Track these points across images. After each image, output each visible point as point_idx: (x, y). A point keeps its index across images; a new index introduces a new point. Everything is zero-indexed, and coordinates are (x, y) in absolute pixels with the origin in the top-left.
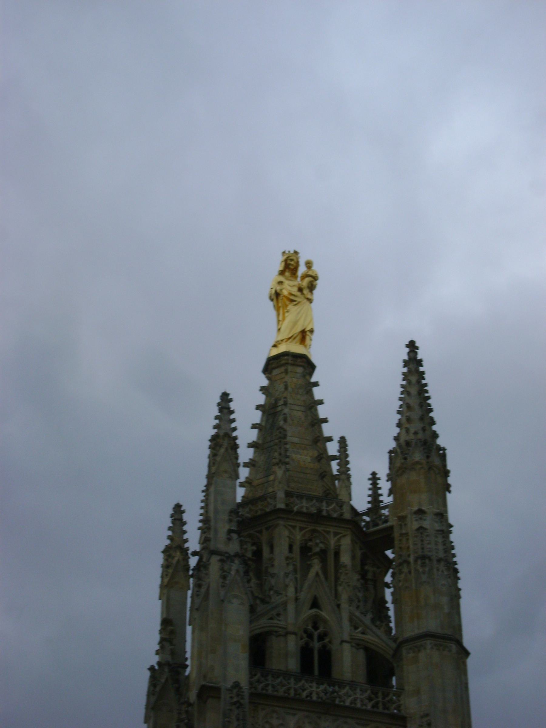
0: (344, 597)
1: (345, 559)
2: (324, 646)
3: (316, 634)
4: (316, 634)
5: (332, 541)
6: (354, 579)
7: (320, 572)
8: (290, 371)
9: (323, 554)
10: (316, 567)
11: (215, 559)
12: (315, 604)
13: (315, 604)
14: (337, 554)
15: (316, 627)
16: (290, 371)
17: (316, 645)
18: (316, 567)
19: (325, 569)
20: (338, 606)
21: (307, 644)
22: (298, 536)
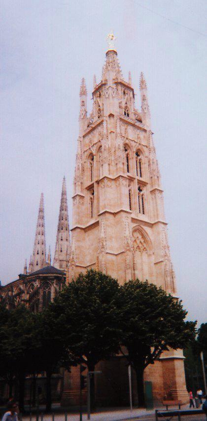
13: (126, 104)
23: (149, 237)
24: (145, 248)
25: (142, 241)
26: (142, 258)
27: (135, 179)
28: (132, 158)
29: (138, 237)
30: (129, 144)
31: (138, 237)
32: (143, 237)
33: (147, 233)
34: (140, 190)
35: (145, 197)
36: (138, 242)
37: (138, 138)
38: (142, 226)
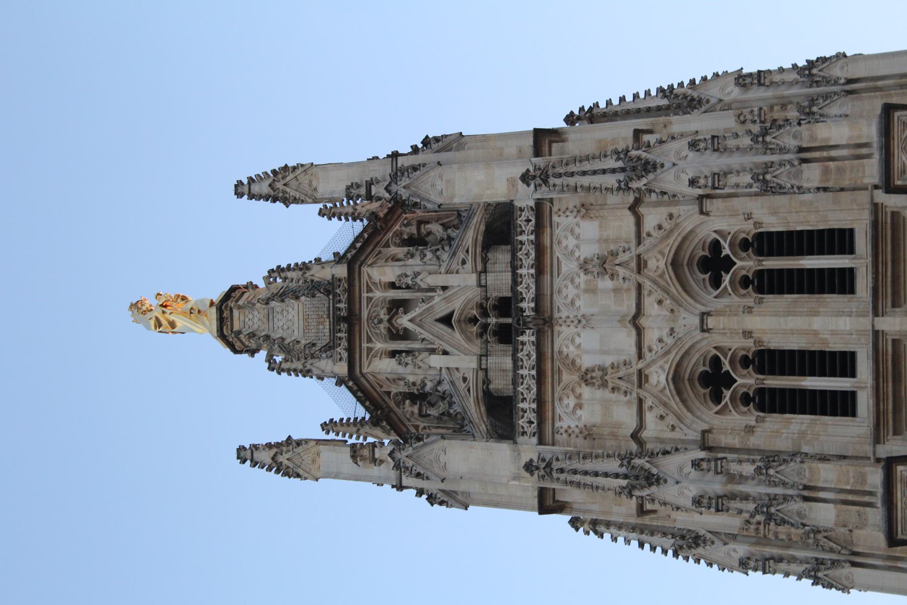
0: (431, 281)
2: (495, 307)
3: (482, 320)
4: (482, 320)
5: (378, 294)
6: (415, 263)
7: (410, 316)
10: (404, 321)
11: (406, 481)
12: (446, 320)
13: (446, 320)
14: (393, 286)
15: (474, 320)
17: (492, 320)
18: (404, 321)
20: (444, 288)
21: (495, 333)
22: (379, 345)
28: (747, 334)
30: (674, 357)
37: (603, 265)
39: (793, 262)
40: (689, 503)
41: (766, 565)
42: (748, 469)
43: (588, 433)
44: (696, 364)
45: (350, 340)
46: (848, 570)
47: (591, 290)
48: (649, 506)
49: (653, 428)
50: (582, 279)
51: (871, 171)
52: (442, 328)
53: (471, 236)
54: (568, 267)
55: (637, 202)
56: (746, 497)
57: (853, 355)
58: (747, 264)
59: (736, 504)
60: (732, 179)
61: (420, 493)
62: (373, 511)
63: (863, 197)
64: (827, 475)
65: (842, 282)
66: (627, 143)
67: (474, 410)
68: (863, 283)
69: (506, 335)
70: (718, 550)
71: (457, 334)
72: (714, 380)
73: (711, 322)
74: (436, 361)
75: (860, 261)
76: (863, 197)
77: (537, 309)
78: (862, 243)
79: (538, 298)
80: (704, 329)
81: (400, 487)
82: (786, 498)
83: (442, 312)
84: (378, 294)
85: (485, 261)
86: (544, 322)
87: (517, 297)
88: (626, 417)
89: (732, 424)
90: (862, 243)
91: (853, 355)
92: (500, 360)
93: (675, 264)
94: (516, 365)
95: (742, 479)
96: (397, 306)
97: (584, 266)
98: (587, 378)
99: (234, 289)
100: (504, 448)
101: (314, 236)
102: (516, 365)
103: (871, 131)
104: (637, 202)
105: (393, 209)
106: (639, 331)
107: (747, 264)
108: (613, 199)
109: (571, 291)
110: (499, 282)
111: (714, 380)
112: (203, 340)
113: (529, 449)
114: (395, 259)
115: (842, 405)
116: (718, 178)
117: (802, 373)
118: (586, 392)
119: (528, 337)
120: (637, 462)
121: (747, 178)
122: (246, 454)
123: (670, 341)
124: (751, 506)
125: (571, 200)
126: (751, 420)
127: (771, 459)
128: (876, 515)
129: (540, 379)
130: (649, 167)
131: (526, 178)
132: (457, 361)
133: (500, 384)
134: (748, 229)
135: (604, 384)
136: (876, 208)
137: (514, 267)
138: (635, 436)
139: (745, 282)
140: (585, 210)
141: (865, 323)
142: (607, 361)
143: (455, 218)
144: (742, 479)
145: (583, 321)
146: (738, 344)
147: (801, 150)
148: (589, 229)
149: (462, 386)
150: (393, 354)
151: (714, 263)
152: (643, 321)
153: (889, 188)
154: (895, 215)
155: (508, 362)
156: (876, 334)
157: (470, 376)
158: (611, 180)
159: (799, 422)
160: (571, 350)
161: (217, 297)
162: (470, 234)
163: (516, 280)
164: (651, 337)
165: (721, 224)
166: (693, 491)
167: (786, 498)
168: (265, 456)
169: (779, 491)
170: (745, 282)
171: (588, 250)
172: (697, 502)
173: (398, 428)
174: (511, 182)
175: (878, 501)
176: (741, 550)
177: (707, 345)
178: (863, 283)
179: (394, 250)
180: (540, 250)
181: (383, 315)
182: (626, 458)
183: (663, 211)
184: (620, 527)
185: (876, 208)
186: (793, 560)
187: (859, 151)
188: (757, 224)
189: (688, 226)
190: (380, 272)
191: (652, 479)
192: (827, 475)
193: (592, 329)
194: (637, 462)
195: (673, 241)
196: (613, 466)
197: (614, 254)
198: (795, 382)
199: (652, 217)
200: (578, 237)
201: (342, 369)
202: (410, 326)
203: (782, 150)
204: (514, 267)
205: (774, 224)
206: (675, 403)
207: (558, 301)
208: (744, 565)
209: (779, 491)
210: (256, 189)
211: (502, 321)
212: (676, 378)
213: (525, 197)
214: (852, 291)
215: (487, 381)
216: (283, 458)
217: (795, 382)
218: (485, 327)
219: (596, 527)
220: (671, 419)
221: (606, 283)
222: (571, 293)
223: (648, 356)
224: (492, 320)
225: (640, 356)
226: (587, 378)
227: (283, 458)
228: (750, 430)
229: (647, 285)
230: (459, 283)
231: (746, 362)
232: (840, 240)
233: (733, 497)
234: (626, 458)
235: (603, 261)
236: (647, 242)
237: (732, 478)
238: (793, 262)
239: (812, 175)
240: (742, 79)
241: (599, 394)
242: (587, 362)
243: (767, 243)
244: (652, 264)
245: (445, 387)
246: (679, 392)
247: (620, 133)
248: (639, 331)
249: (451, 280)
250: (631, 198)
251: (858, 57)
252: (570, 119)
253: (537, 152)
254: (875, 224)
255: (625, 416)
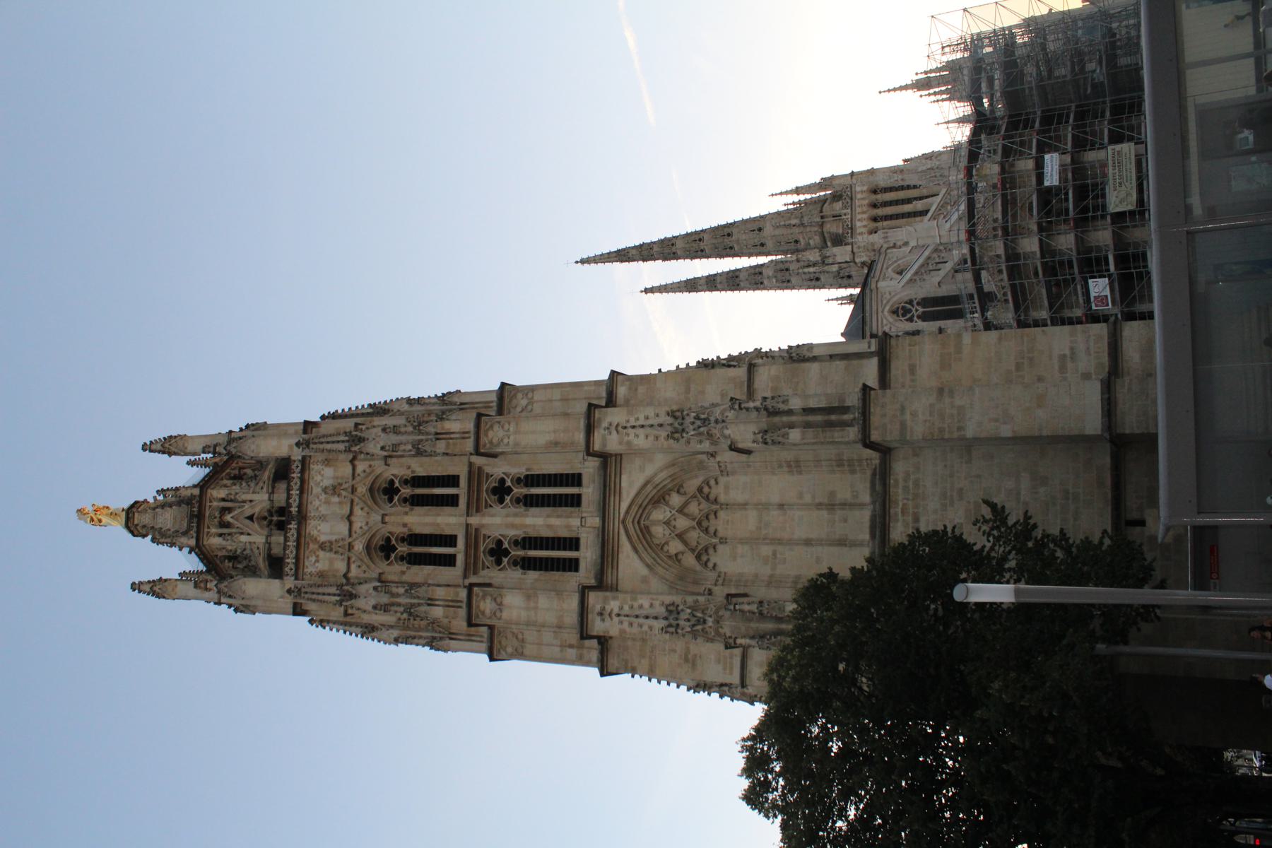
0: (244, 497)
1: (222, 493)
5: (215, 504)
6: (236, 488)
8: (136, 519)
9: (224, 510)
10: (228, 518)
12: (251, 518)
13: (251, 518)
14: (223, 500)
15: (265, 518)
16: (136, 519)
18: (228, 518)
19: (229, 510)
22: (213, 530)
23: (656, 474)
24: (700, 490)
25: (676, 500)
26: (744, 506)
27: (467, 525)
28: (405, 525)
29: (667, 523)
30: (367, 536)
31: (667, 523)
32: (660, 499)
33: (645, 485)
34: (501, 491)
35: (521, 471)
36: (682, 523)
37: (334, 490)
38: (624, 506)
39: (429, 491)
40: (370, 609)
41: (407, 640)
42: (401, 590)
43: (321, 575)
44: (379, 541)
45: (198, 527)
46: (447, 641)
47: (327, 502)
48: (350, 611)
49: (354, 572)
50: (323, 497)
51: (469, 445)
52: (248, 522)
53: (267, 474)
54: (317, 490)
55: (354, 458)
56: (399, 605)
57: (455, 537)
58: (406, 491)
59: (394, 608)
60: (402, 447)
61: (230, 606)
62: (205, 617)
63: (465, 459)
64: (440, 593)
65: (452, 501)
66: (352, 430)
67: (262, 563)
68: (463, 501)
69: (281, 526)
70: (385, 634)
71: (256, 525)
72: (387, 549)
73: (387, 519)
74: (244, 538)
75: (461, 491)
76: (465, 459)
77: (299, 512)
78: (463, 482)
79: (300, 506)
80: (383, 522)
81: (219, 603)
82: (419, 605)
83: (248, 513)
84: (215, 504)
85: (273, 487)
86: (302, 517)
87: (289, 505)
88: (341, 566)
89: (394, 570)
90: (463, 482)
91: (455, 537)
92: (278, 538)
93: (371, 490)
94: (286, 539)
95: (398, 595)
96: (224, 510)
97: (325, 490)
98: (322, 547)
99: (136, 502)
100: (276, 583)
101: (182, 473)
102: (286, 539)
103: (470, 426)
104: (354, 458)
105: (228, 459)
106: (351, 524)
107: (406, 491)
108: (342, 456)
109: (317, 503)
110: (280, 498)
111: (387, 549)
112: (117, 529)
113: (290, 582)
114: (225, 486)
115: (449, 561)
116: (395, 447)
117: (431, 545)
118: (321, 554)
119: (293, 526)
120: (345, 588)
121: (410, 447)
122: (135, 587)
123: (365, 528)
124: (402, 609)
125: (320, 457)
126: (404, 568)
127: (413, 585)
128: (462, 612)
129: (298, 547)
130: (361, 440)
131: (298, 444)
132: (254, 539)
133: (277, 550)
134: (408, 474)
135: (331, 550)
136: (471, 464)
137: (289, 489)
138: (345, 576)
139: (405, 500)
140: (327, 462)
141: (462, 520)
142: (333, 538)
143: (260, 464)
144: (398, 595)
145: (323, 518)
146: (399, 530)
147: (437, 434)
148: (329, 472)
149: (256, 552)
150: (220, 535)
151: (390, 491)
152: (353, 518)
153: (477, 452)
154: (480, 468)
155: (281, 539)
156: (467, 525)
157: (261, 547)
158: (341, 447)
159: (428, 569)
160: (315, 533)
161: (126, 506)
162: (267, 473)
163: (289, 497)
164: (356, 526)
165: (395, 471)
166: (373, 602)
167: (419, 605)
168: (147, 588)
169: (416, 601)
170: (405, 500)
171: (327, 482)
172: (375, 607)
173: (221, 575)
174: (290, 447)
175: (464, 605)
176: (395, 633)
177: (385, 531)
178: (463, 501)
179: (225, 482)
180: (302, 481)
181: (217, 514)
182: (340, 586)
183: (367, 463)
184: (335, 623)
185: (471, 464)
186: (421, 637)
187: (464, 435)
188: (413, 472)
189: (378, 471)
190: (218, 493)
191: (352, 596)
192: (440, 593)
193: (326, 522)
194: (345, 588)
195: (371, 479)
196: (333, 590)
197: (340, 484)
198: (426, 550)
199: (361, 467)
200: (322, 476)
201: (193, 542)
202: (231, 520)
203: (427, 434)
204: (289, 489)
205: (421, 472)
206: (366, 559)
207: (310, 508)
208: (397, 641)
209: (416, 601)
210: (154, 447)
211: (279, 519)
212: (368, 547)
213: (297, 455)
214: (457, 505)
215: (270, 549)
216: (157, 588)
217: (426, 550)
218: (271, 521)
219: (322, 623)
220: (364, 567)
221: (335, 499)
222: (317, 503)
223: (354, 536)
224: (275, 518)
225: (350, 536)
226: (322, 547)
227: (157, 588)
228: (403, 573)
229: (356, 500)
230: (259, 498)
231: (403, 540)
232: (452, 481)
233: (393, 604)
234: (340, 586)
235: (334, 488)
236: (358, 479)
237: (393, 595)
238: (429, 491)
239: (441, 446)
240: (409, 401)
241: (328, 555)
242: (323, 538)
243: (417, 481)
244: (359, 490)
245: (248, 552)
246: (369, 554)
247: (349, 424)
248: (351, 524)
249: (255, 497)
250: (351, 456)
251: (465, 393)
252: (323, 417)
253: (305, 432)
254: (470, 473)
255: (341, 566)
